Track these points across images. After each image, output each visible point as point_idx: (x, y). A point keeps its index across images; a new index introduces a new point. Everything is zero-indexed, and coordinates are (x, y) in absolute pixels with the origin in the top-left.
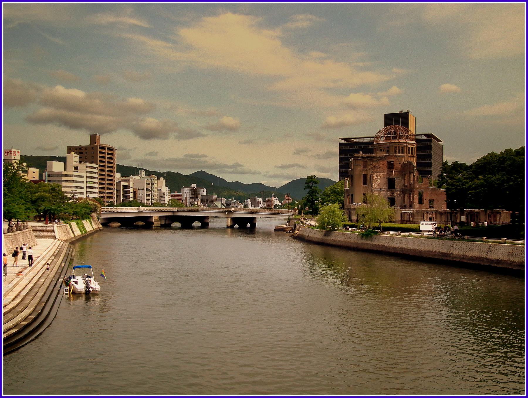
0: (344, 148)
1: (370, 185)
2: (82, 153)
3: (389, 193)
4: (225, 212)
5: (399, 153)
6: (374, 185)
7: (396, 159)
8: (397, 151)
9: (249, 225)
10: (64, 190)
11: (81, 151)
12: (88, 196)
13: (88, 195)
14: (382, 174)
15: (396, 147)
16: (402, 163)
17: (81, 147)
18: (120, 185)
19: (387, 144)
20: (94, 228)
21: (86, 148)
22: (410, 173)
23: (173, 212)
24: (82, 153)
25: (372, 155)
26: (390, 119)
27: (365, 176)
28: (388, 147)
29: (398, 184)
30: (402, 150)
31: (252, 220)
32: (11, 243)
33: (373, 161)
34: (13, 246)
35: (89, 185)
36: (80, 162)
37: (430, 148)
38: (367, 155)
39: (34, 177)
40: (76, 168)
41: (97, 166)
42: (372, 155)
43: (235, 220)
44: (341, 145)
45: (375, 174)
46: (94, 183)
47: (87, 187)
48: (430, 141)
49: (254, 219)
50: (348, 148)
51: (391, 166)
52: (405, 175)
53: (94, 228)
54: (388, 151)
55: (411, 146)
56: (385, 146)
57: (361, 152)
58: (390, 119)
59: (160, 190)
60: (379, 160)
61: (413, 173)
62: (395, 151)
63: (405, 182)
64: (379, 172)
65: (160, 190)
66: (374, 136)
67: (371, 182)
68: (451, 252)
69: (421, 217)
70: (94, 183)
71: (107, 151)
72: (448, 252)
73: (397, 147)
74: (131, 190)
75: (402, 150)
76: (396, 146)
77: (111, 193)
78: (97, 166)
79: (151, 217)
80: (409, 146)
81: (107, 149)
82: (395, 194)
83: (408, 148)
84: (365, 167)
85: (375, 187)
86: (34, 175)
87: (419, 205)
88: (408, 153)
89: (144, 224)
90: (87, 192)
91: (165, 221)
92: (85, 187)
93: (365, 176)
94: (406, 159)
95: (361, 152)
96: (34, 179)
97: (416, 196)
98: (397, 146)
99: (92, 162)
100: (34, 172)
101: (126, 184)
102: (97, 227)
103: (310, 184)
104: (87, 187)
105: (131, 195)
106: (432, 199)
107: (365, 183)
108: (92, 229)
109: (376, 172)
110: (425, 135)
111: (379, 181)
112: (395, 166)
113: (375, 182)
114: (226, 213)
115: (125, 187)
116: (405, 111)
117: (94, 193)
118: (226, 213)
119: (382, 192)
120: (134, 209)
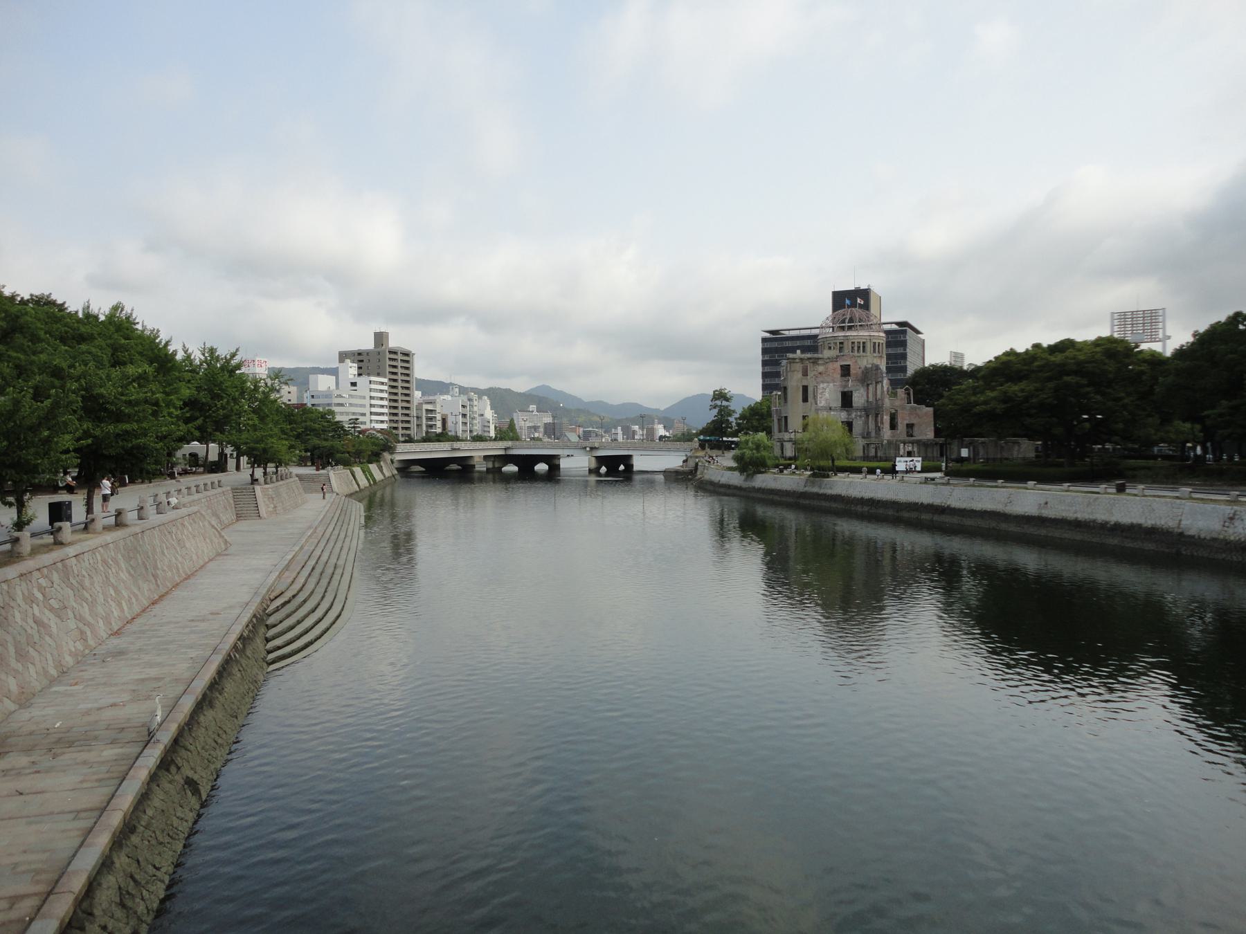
0: (768, 345)
1: (813, 401)
2: (362, 361)
3: (843, 415)
4: (585, 448)
6: (821, 402)
7: (854, 361)
9: (622, 467)
10: (338, 418)
11: (360, 358)
13: (373, 425)
14: (831, 384)
15: (853, 343)
16: (863, 367)
17: (360, 352)
18: (421, 410)
19: (840, 338)
20: (387, 476)
21: (368, 353)
22: (877, 383)
23: (506, 449)
24: (362, 361)
25: (816, 355)
26: (840, 299)
27: (805, 389)
28: (841, 343)
29: (859, 399)
30: (864, 347)
31: (627, 460)
32: (271, 500)
33: (818, 364)
34: (273, 504)
35: (374, 410)
36: (360, 375)
37: (903, 344)
38: (809, 355)
39: (290, 400)
40: (354, 384)
41: (385, 380)
42: (816, 355)
43: (601, 460)
44: (764, 340)
45: (822, 385)
46: (382, 406)
47: (371, 413)
48: (905, 332)
49: (630, 457)
50: (776, 345)
51: (846, 371)
52: (868, 385)
53: (387, 476)
54: (841, 349)
55: (877, 341)
56: (835, 341)
57: (798, 351)
58: (840, 299)
59: (482, 415)
60: (827, 363)
61: (882, 382)
63: (868, 397)
64: (828, 382)
65: (482, 415)
66: (819, 326)
67: (815, 397)
68: (948, 503)
71: (400, 357)
72: (943, 505)
73: (856, 344)
74: (439, 417)
75: (864, 347)
76: (853, 341)
77: (408, 422)
78: (385, 380)
79: (470, 457)
80: (874, 341)
82: (853, 416)
83: (872, 344)
84: (805, 374)
85: (822, 405)
86: (290, 396)
87: (892, 433)
88: (872, 351)
91: (494, 462)
92: (368, 414)
93: (805, 389)
94: (870, 361)
95: (798, 351)
96: (290, 403)
97: (887, 418)
98: (856, 341)
99: (378, 375)
101: (430, 407)
102: (391, 475)
103: (718, 403)
104: (371, 413)
105: (439, 424)
106: (912, 422)
107: (805, 399)
108: (382, 478)
109: (823, 382)
110: (897, 324)
111: (827, 395)
112: (853, 371)
113: (821, 397)
114: (588, 449)
115: (427, 411)
116: (863, 287)
117: (382, 422)
118: (588, 449)
119: (832, 413)
120: (446, 446)
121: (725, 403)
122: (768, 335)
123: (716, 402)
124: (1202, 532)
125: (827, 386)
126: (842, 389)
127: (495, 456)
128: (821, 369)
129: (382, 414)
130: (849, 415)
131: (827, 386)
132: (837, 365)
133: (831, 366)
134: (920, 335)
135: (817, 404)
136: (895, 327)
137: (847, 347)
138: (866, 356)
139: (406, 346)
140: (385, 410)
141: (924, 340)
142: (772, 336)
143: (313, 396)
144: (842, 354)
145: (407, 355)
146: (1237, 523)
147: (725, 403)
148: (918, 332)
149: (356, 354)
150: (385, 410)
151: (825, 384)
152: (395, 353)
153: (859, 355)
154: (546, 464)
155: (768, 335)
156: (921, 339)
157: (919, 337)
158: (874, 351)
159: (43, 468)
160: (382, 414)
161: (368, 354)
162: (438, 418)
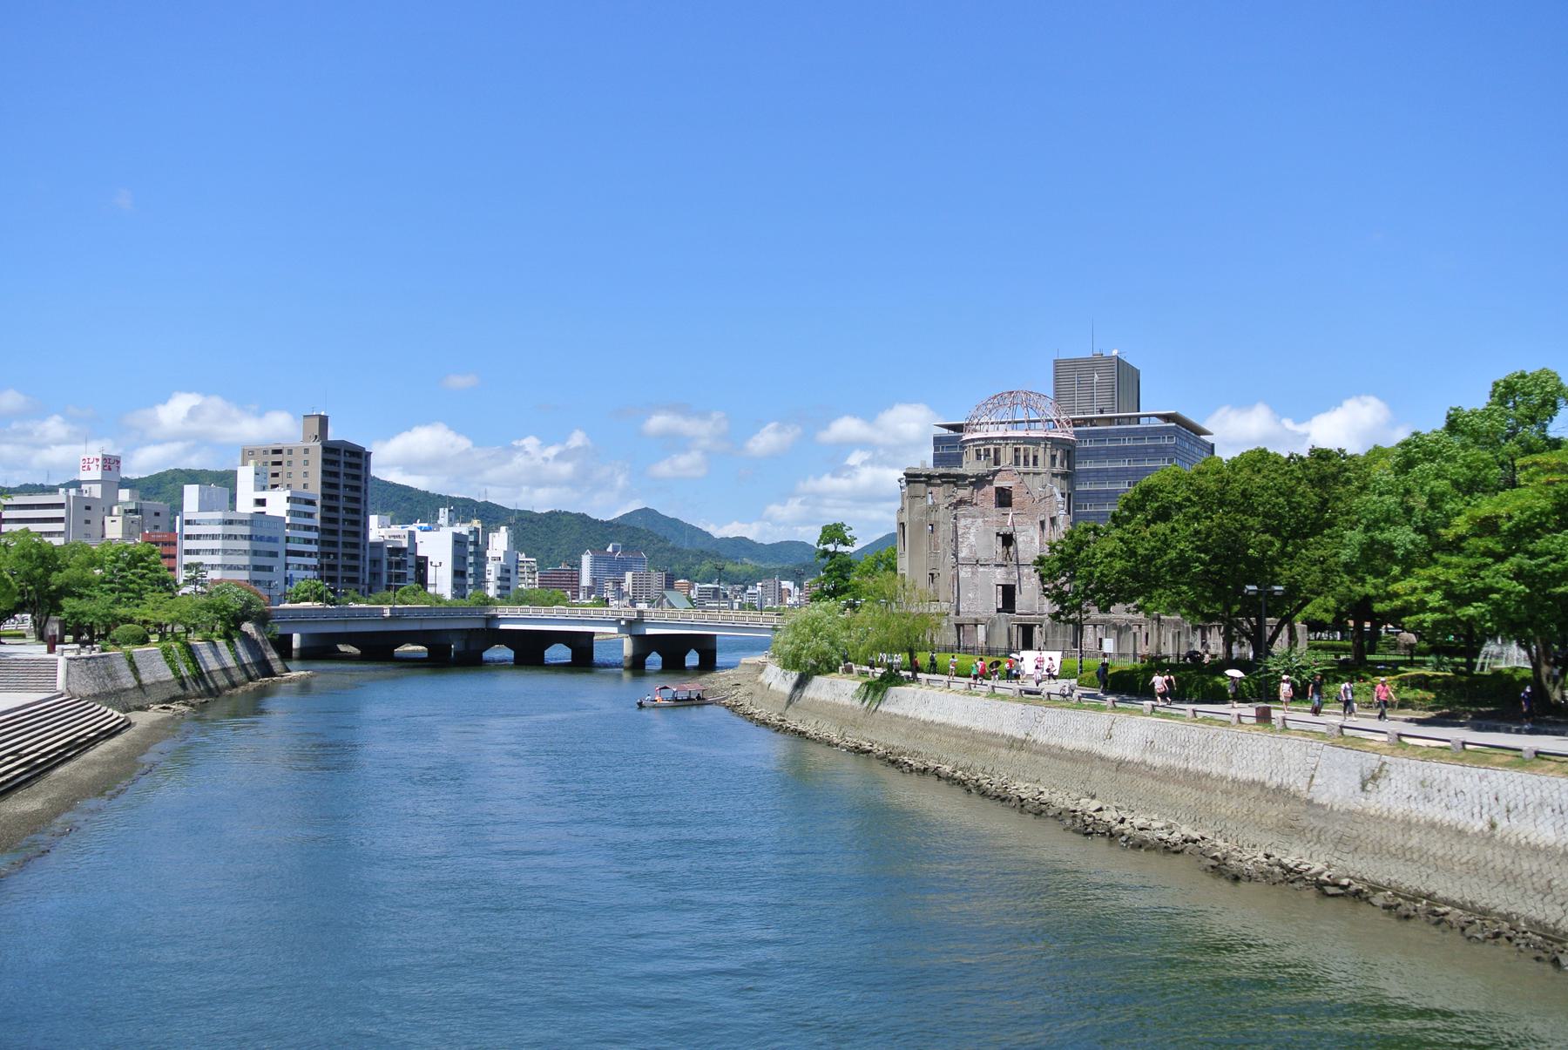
2: (279, 463)
5: (1026, 463)
8: (1022, 458)
11: (277, 458)
12: (291, 575)
13: (289, 572)
14: (980, 521)
24: (279, 463)
26: (1068, 373)
39: (156, 527)
40: (261, 502)
44: (938, 441)
46: (309, 541)
47: (289, 553)
54: (997, 462)
56: (987, 447)
58: (1068, 373)
62: (1017, 458)
64: (974, 517)
69: (1065, 637)
70: (309, 541)
74: (411, 561)
81: (345, 451)
89: (358, 652)
90: (287, 566)
92: (282, 554)
100: (157, 514)
104: (289, 553)
109: (965, 516)
111: (972, 539)
112: (1015, 499)
114: (623, 623)
117: (306, 568)
119: (981, 569)
121: (841, 548)
122: (945, 431)
123: (827, 546)
124: (1336, 800)
125: (973, 523)
126: (996, 530)
128: (963, 493)
129: (310, 555)
130: (1009, 574)
131: (973, 523)
132: (990, 490)
136: (1160, 423)
137: (1007, 455)
138: (1039, 474)
140: (314, 548)
141: (1213, 445)
143: (188, 522)
144: (998, 468)
146: (1383, 783)
147: (841, 548)
148: (1199, 431)
149: (270, 452)
150: (314, 548)
153: (1026, 470)
154: (568, 645)
156: (1207, 443)
157: (1204, 441)
160: (310, 555)
161: (290, 452)
162: (409, 563)
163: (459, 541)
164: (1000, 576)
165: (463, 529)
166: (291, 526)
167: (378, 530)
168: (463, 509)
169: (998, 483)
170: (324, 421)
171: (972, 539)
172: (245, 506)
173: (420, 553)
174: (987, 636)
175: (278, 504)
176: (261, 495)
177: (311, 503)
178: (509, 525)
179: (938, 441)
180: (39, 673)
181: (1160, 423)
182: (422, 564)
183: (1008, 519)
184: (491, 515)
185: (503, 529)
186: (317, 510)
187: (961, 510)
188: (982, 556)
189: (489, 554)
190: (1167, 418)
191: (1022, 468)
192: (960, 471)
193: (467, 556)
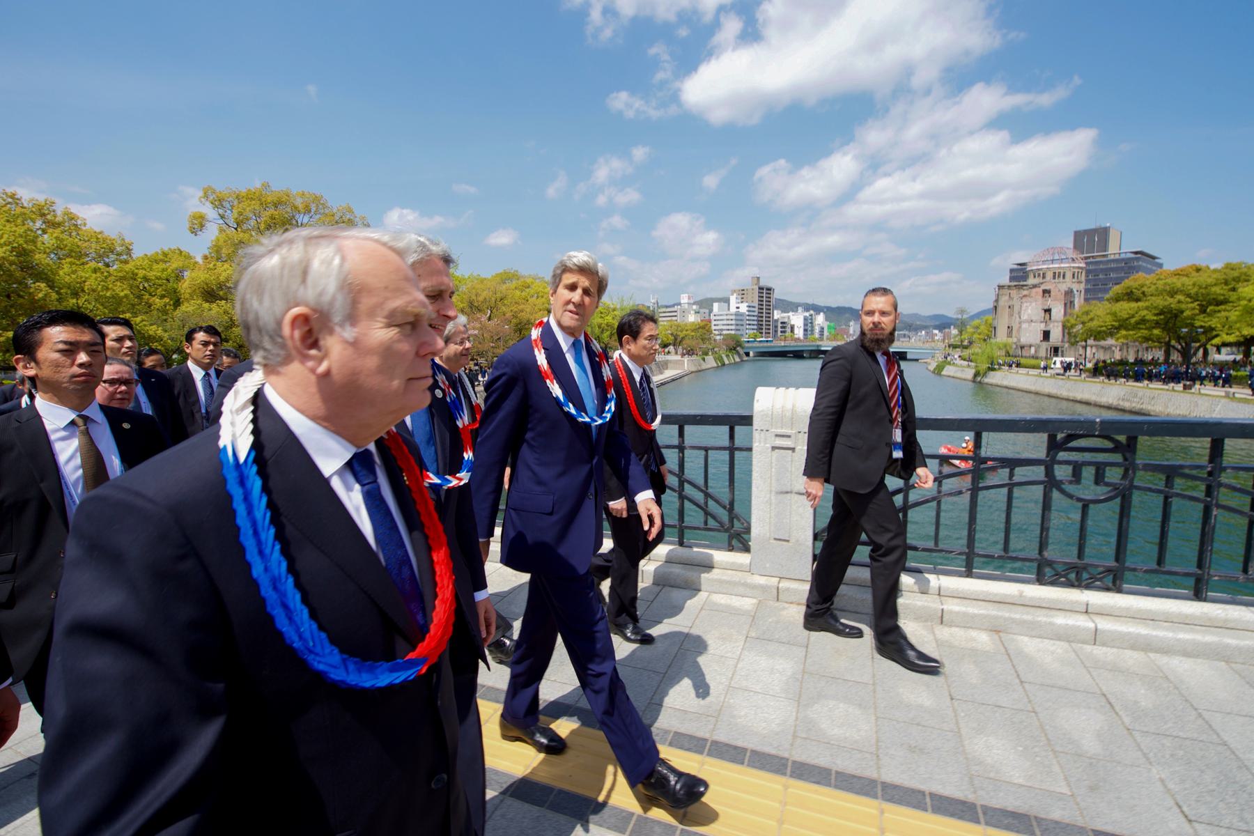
1: (1017, 316)
15: (1055, 273)
40: (738, 308)
44: (1012, 271)
54: (1044, 277)
74: (789, 326)
82: (1051, 326)
111: (1029, 311)
112: (1052, 293)
119: (1033, 324)
127: (812, 351)
128: (1025, 292)
132: (1040, 290)
133: (1034, 290)
134: (1157, 260)
135: (1020, 318)
136: (1133, 256)
137: (1049, 275)
139: (770, 285)
142: (1019, 267)
145: (769, 289)
148: (1153, 258)
151: (1028, 304)
152: (763, 289)
155: (1016, 267)
158: (1074, 277)
159: (471, 365)
163: (805, 319)
164: (1043, 327)
165: (807, 314)
166: (748, 315)
167: (777, 315)
168: (807, 308)
169: (1043, 287)
170: (758, 278)
171: (1029, 311)
172: (733, 310)
173: (792, 323)
174: (1036, 351)
175: (744, 308)
176: (738, 305)
177: (754, 307)
178: (824, 313)
179: (1012, 271)
180: (681, 363)
181: (1133, 256)
182: (792, 328)
183: (1049, 303)
184: (818, 309)
185: (822, 314)
186: (756, 309)
187: (1024, 300)
188: (1034, 319)
189: (817, 323)
190: (1136, 253)
191: (1057, 280)
192: (1025, 283)
193: (808, 324)
